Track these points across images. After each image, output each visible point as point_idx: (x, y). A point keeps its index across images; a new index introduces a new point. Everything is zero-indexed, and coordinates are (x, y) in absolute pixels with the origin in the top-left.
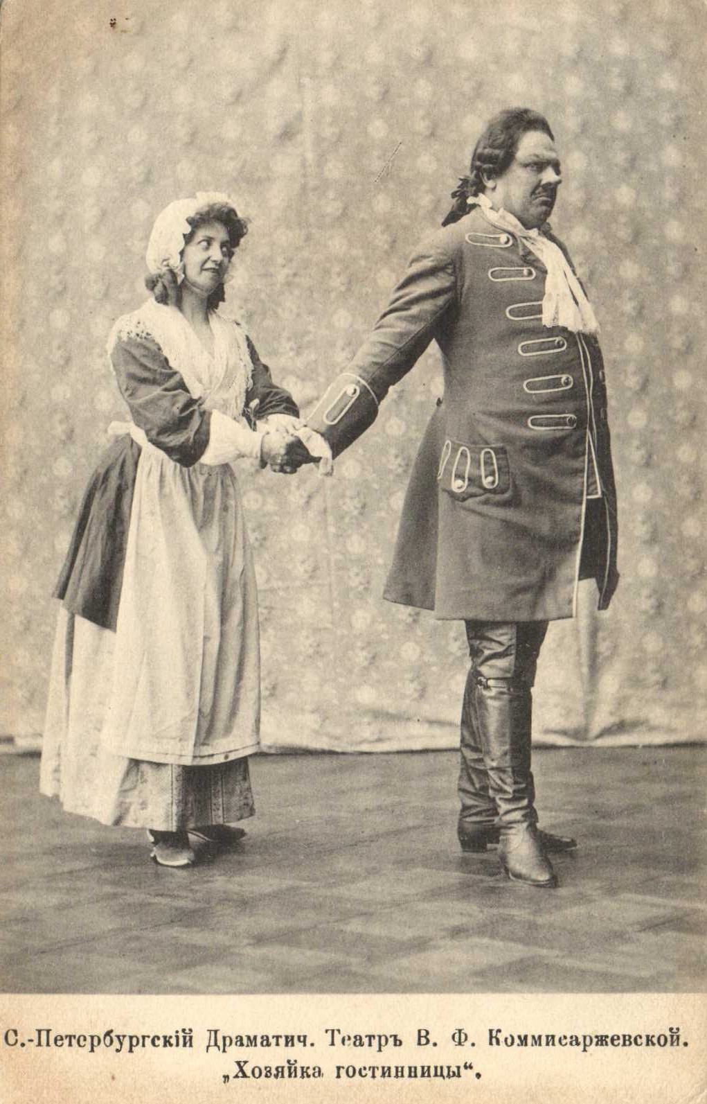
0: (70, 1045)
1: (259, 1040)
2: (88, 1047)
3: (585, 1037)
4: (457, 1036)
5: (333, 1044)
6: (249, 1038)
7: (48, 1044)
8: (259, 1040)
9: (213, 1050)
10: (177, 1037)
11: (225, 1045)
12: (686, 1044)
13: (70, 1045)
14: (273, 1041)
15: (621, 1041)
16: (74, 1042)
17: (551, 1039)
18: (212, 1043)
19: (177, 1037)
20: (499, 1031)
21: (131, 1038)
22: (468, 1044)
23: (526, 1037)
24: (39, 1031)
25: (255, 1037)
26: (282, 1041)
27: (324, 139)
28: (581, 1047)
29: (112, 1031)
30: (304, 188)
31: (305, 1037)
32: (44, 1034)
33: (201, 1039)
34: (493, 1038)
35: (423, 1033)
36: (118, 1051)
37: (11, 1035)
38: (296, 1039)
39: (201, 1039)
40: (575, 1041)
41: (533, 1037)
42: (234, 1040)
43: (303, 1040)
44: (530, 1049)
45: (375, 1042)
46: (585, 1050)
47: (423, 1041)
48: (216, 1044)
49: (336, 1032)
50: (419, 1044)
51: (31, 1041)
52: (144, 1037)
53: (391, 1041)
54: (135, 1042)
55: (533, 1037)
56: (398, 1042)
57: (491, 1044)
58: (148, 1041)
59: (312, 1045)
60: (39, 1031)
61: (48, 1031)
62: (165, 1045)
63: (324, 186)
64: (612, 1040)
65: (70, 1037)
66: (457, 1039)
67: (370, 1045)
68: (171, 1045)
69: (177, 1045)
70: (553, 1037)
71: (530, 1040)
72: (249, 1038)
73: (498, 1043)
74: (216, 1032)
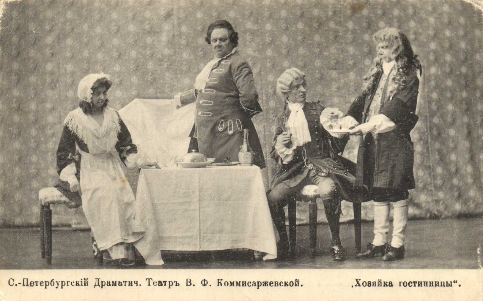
0: (37, 285)
1: (117, 283)
2: (44, 286)
3: (258, 282)
5: (149, 285)
6: (113, 282)
7: (27, 285)
8: (117, 283)
12: (302, 286)
13: (37, 285)
14: (123, 284)
15: (274, 284)
16: (39, 284)
18: (97, 284)
20: (222, 280)
21: (62, 282)
22: (208, 285)
23: (233, 282)
25: (116, 282)
27: (180, 18)
28: (257, 287)
30: (174, 36)
32: (25, 281)
33: (92, 282)
34: (219, 283)
35: (189, 280)
36: (57, 288)
37: (11, 281)
38: (133, 283)
39: (92, 282)
41: (237, 282)
42: (106, 283)
44: (235, 288)
45: (167, 283)
46: (258, 288)
47: (189, 284)
48: (98, 285)
50: (187, 285)
51: (19, 284)
53: (175, 284)
54: (63, 284)
55: (237, 282)
56: (177, 284)
61: (27, 279)
63: (180, 35)
64: (270, 284)
67: (165, 285)
68: (79, 285)
71: (235, 283)
72: (113, 282)
73: (221, 285)
74: (98, 279)
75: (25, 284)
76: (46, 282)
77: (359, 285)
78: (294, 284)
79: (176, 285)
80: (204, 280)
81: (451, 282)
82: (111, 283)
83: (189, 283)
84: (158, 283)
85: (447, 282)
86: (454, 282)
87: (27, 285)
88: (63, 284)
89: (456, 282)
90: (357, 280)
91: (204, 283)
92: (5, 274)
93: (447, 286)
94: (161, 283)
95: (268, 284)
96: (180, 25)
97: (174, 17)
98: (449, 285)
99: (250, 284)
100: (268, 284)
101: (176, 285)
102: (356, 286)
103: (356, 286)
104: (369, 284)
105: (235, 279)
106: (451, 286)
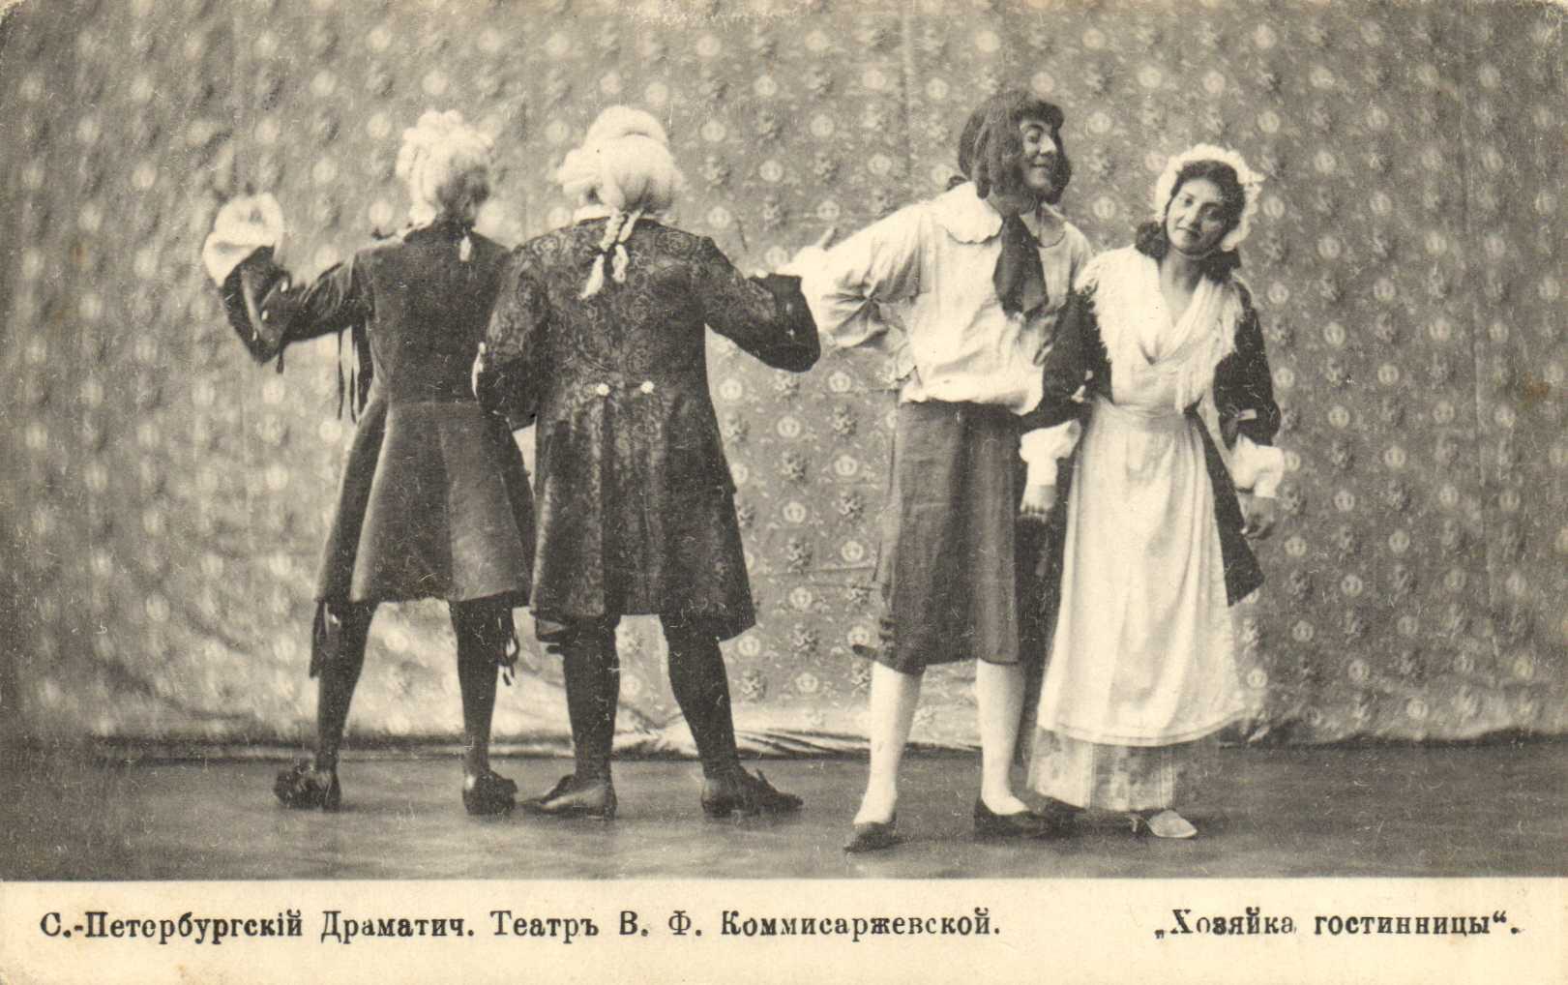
0: (133, 934)
1: (396, 927)
3: (856, 921)
4: (675, 924)
5: (500, 932)
6: (381, 922)
8: (396, 927)
9: (331, 939)
10: (280, 921)
11: (347, 933)
13: (133, 934)
14: (416, 929)
16: (138, 930)
17: (808, 927)
18: (330, 929)
19: (280, 921)
20: (735, 914)
23: (773, 921)
24: (90, 915)
26: (429, 928)
28: (851, 934)
29: (189, 915)
30: (903, 108)
31: (460, 921)
32: (96, 919)
33: (313, 923)
35: (628, 917)
36: (198, 941)
37: (51, 920)
38: (448, 925)
39: (313, 923)
40: (841, 927)
43: (458, 925)
45: (561, 930)
47: (628, 927)
48: (335, 932)
49: (505, 917)
50: (623, 932)
51: (79, 928)
52: (234, 922)
53: (583, 928)
54: (221, 929)
56: (591, 929)
57: (724, 932)
58: (240, 928)
59: (471, 933)
60: (90, 915)
61: (103, 915)
62: (263, 934)
64: (895, 925)
65: (132, 923)
66: (675, 924)
67: (553, 933)
68: (272, 933)
69: (281, 933)
70: (812, 921)
72: (381, 922)
74: (335, 914)
75: (96, 929)
76: (163, 923)
77: (1186, 930)
78: (974, 927)
79: (588, 933)
80: (679, 914)
81: (1486, 919)
82: (376, 927)
83: (629, 923)
84: (529, 926)
85: (1473, 919)
86: (1496, 919)
87: (102, 934)
88: (221, 929)
89: (1503, 919)
90: (1177, 913)
91: (679, 923)
92: (31, 898)
93: (1472, 931)
94: (408, 925)
95: (890, 926)
96: (923, 74)
97: (906, 51)
98: (1480, 927)
99: (827, 928)
100: (890, 926)
101: (588, 933)
102: (1174, 932)
103: (1174, 932)
104: (1219, 926)
105: (777, 912)
106: (1486, 931)
